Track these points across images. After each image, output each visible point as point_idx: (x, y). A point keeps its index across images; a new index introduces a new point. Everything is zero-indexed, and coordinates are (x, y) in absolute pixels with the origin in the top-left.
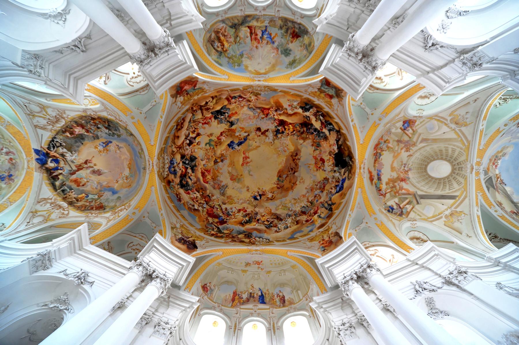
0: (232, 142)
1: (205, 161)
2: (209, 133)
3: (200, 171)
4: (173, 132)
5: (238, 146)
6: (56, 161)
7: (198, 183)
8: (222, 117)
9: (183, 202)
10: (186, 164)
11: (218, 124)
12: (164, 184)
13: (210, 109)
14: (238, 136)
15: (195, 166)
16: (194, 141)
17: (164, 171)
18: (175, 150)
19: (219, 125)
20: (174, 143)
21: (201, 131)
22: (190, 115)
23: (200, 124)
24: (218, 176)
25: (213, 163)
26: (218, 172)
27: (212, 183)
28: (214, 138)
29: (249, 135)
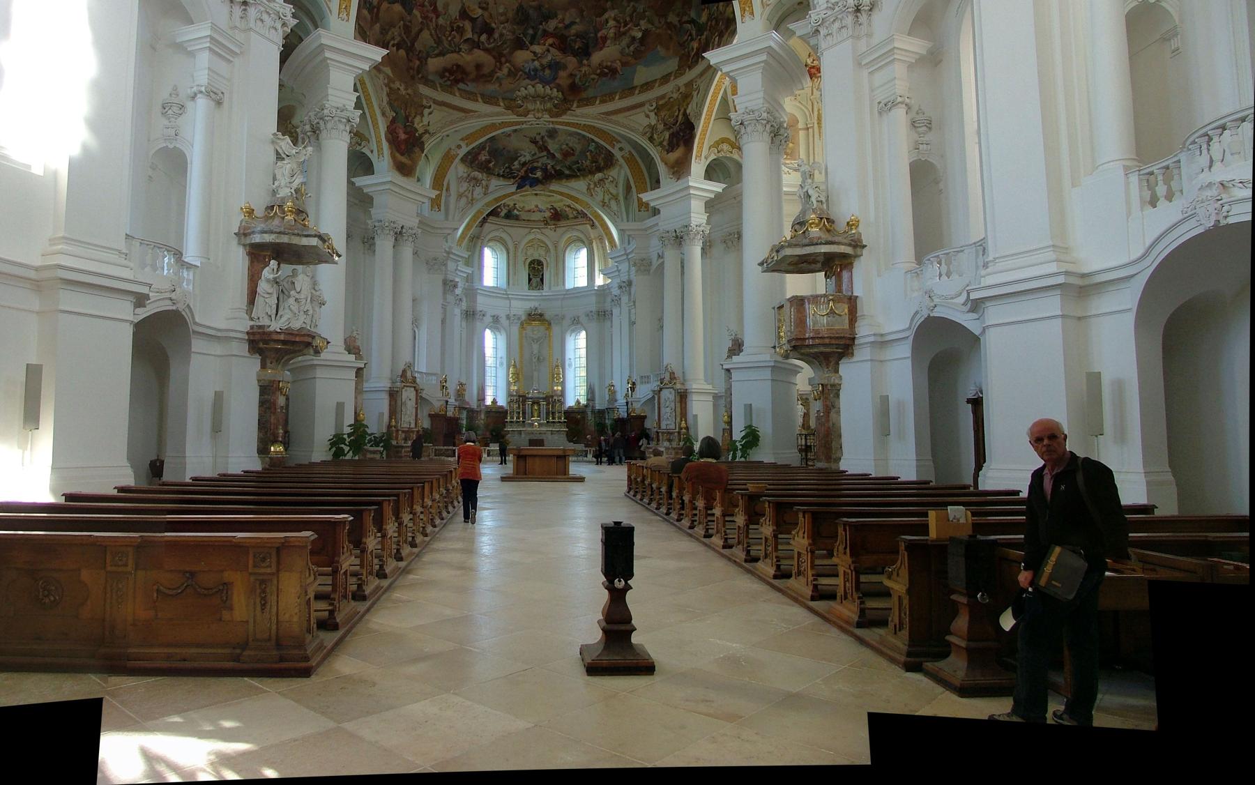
4: (471, 87)
6: (533, 170)
9: (618, 65)
15: (539, 8)
17: (551, 99)
18: (505, 71)
21: (454, 11)
22: (434, 64)
23: (441, 21)
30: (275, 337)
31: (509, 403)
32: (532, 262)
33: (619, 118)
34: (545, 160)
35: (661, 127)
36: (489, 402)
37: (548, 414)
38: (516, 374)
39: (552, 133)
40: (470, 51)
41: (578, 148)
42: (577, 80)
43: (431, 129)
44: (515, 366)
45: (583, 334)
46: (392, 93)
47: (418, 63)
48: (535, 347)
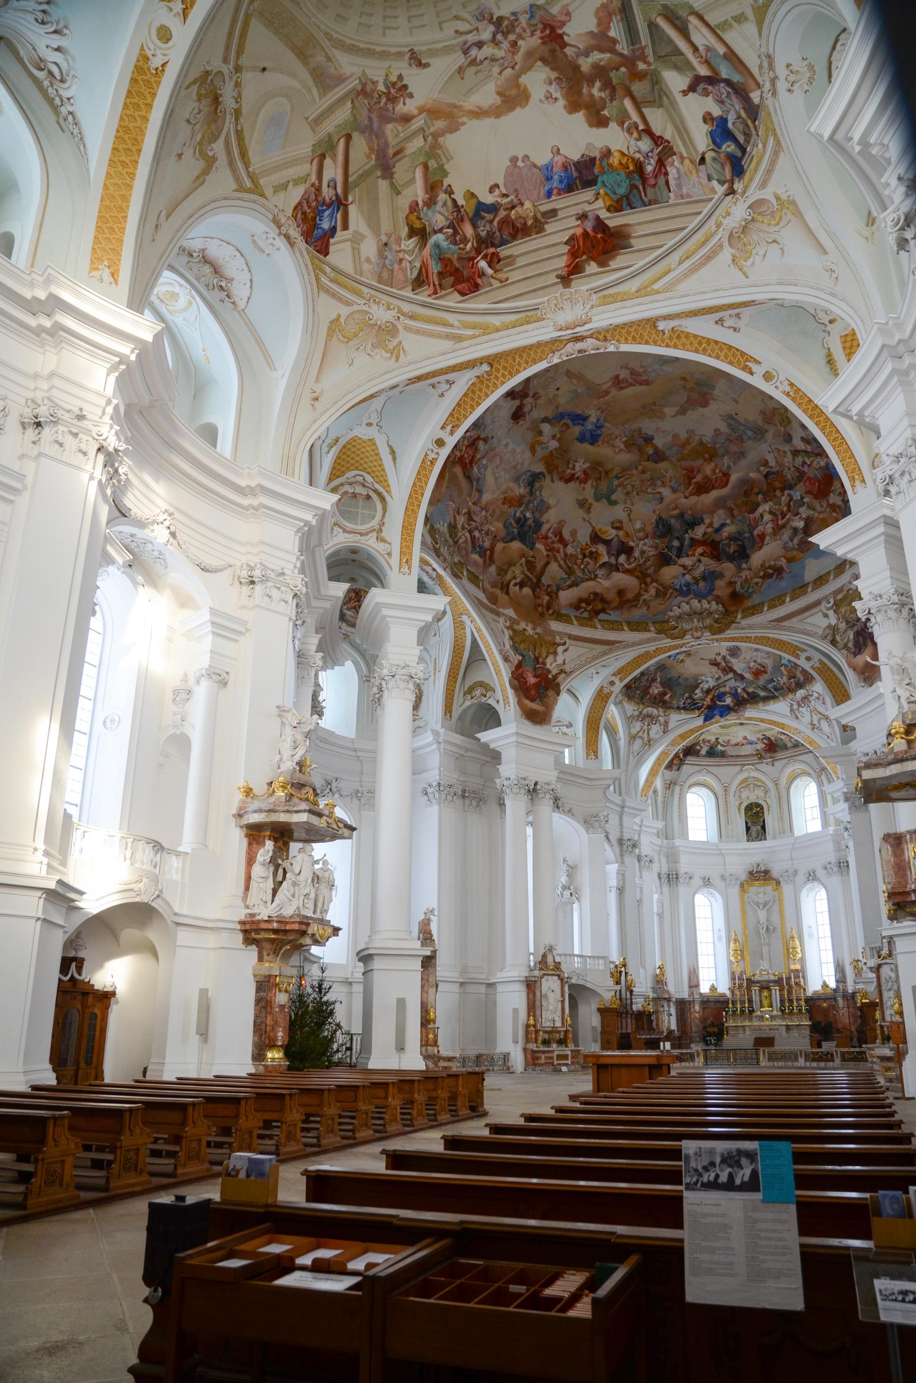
0: (582, 439)
1: (661, 490)
2: (581, 513)
3: (694, 499)
4: (614, 616)
5: (585, 419)
6: (721, 696)
7: (730, 504)
8: (528, 515)
9: (783, 562)
10: (682, 545)
11: (549, 508)
12: (739, 616)
13: (528, 562)
14: (559, 440)
15: (681, 516)
16: (615, 542)
17: (710, 613)
18: (652, 591)
19: (551, 502)
20: (638, 596)
21: (584, 537)
22: (566, 596)
23: (570, 550)
24: (701, 443)
25: (663, 465)
26: (687, 442)
27: (726, 460)
28: (589, 492)
29: (545, 420)
30: (263, 926)
31: (732, 991)
32: (749, 808)
33: (794, 622)
34: (732, 683)
35: (843, 626)
36: (705, 988)
37: (782, 1001)
38: (741, 953)
39: (734, 652)
40: (608, 576)
41: (769, 663)
42: (738, 588)
43: (567, 668)
44: (736, 940)
45: (822, 894)
46: (518, 638)
47: (546, 598)
48: (762, 915)
